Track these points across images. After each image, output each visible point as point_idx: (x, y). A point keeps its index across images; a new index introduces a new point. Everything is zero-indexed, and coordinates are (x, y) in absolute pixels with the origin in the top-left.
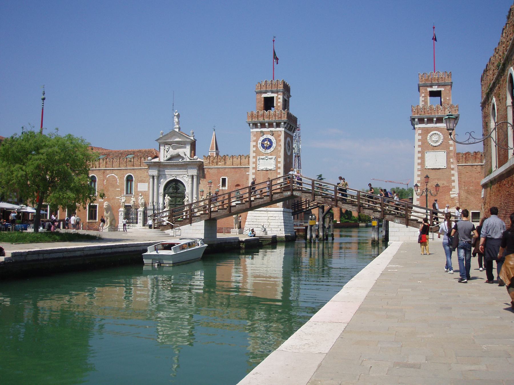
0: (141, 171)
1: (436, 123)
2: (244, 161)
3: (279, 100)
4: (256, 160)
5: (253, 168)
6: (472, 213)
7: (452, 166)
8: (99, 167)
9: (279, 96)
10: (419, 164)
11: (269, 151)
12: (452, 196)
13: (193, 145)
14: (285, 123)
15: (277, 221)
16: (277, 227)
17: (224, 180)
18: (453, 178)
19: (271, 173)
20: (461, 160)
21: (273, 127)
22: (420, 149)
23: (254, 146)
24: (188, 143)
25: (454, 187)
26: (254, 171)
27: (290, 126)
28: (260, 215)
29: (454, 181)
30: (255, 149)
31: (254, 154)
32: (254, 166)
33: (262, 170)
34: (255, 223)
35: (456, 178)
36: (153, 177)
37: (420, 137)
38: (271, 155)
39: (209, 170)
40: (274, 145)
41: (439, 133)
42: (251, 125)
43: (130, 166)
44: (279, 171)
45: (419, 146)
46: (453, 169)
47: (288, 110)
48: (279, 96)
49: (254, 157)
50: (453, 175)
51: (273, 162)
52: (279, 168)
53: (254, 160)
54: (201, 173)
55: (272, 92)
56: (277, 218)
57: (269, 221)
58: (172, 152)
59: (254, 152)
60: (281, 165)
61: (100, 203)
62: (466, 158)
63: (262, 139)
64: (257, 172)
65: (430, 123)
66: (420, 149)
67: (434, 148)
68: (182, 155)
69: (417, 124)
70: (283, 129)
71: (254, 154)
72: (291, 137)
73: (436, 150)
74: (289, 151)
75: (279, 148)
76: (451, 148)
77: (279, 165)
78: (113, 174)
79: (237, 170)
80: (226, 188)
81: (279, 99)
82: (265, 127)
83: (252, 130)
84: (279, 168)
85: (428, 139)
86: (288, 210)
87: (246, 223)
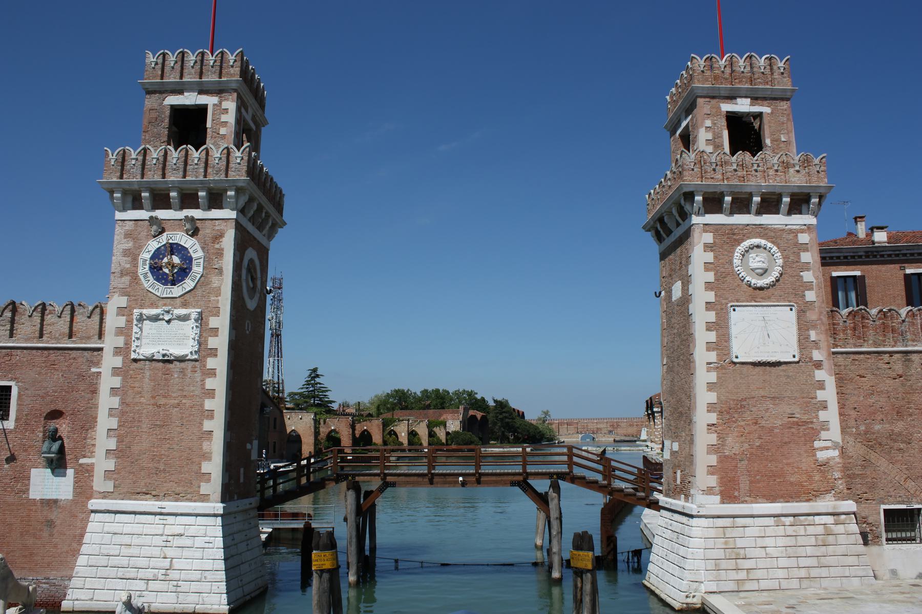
1: (759, 213)
3: (224, 118)
4: (129, 322)
5: (117, 351)
6: (885, 510)
7: (817, 355)
9: (225, 105)
10: (710, 347)
11: (177, 291)
12: (822, 456)
14: (239, 191)
15: (198, 554)
16: (196, 575)
18: (821, 395)
19: (183, 372)
20: (842, 336)
21: (197, 207)
22: (711, 296)
25: (825, 426)
26: (118, 362)
27: (260, 208)
28: (137, 529)
29: (824, 406)
31: (123, 301)
32: (120, 342)
33: (151, 360)
34: (114, 561)
35: (829, 395)
37: (710, 257)
38: (185, 305)
40: (197, 269)
41: (769, 245)
42: (117, 195)
44: (211, 363)
45: (709, 286)
46: (818, 365)
47: (255, 147)
48: (225, 105)
49: (121, 311)
50: (821, 385)
51: (190, 329)
52: (213, 353)
53: (122, 321)
55: (203, 90)
56: (199, 542)
57: (170, 552)
60: (221, 342)
62: (854, 329)
63: (153, 245)
65: (740, 212)
66: (711, 296)
67: (758, 295)
69: (698, 214)
70: (233, 214)
71: (123, 301)
72: (263, 253)
73: (764, 299)
74: (251, 298)
75: (215, 281)
76: (810, 296)
77: (212, 342)
79: (53, 356)
81: (223, 114)
82: (167, 205)
83: (119, 215)
84: (213, 353)
85: (736, 261)
86: (245, 503)
87: (82, 560)
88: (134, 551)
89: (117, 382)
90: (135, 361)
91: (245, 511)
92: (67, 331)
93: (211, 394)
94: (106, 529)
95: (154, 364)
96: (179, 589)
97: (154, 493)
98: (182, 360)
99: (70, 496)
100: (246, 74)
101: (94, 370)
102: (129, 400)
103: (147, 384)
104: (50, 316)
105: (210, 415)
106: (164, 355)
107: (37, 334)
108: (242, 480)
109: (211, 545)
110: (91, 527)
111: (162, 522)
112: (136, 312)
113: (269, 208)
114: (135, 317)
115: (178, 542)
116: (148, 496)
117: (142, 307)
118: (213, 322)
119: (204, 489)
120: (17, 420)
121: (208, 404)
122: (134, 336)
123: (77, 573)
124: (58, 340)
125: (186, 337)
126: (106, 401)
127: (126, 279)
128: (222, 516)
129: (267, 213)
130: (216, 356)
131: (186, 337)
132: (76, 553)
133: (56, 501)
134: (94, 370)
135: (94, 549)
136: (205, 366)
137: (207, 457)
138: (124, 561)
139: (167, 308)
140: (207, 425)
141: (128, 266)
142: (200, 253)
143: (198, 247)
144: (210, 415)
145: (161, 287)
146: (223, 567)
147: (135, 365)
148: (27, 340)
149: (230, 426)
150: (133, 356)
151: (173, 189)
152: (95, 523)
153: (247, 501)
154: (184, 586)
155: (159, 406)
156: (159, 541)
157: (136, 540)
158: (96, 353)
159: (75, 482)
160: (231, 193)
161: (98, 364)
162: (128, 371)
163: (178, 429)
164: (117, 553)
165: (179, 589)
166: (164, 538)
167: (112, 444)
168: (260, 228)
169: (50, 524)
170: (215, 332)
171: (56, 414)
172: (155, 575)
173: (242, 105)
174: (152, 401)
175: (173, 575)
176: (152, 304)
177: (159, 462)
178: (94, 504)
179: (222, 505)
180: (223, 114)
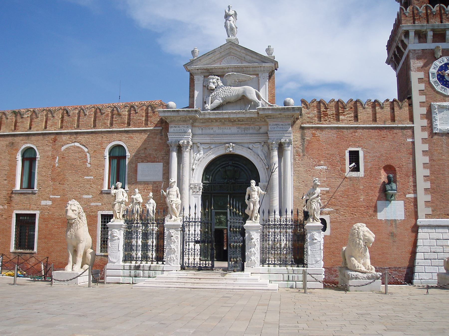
17: (354, 156)
23: (420, 80)
30: (422, 86)
31: (423, 98)
39: (318, 133)
58: (225, 91)
59: (421, 92)
61: (42, 209)
78: (77, 144)
79: (384, 132)
80: (361, 173)
89: (426, 147)
90: (436, 133)
92: (389, 116)
94: (431, 237)
102: (434, 158)
120: (365, 171)
123: (418, 263)
124: (385, 122)
126: (421, 159)
135: (428, 249)
147: (436, 137)
159: (406, 209)
167: (428, 185)
169: (392, 235)
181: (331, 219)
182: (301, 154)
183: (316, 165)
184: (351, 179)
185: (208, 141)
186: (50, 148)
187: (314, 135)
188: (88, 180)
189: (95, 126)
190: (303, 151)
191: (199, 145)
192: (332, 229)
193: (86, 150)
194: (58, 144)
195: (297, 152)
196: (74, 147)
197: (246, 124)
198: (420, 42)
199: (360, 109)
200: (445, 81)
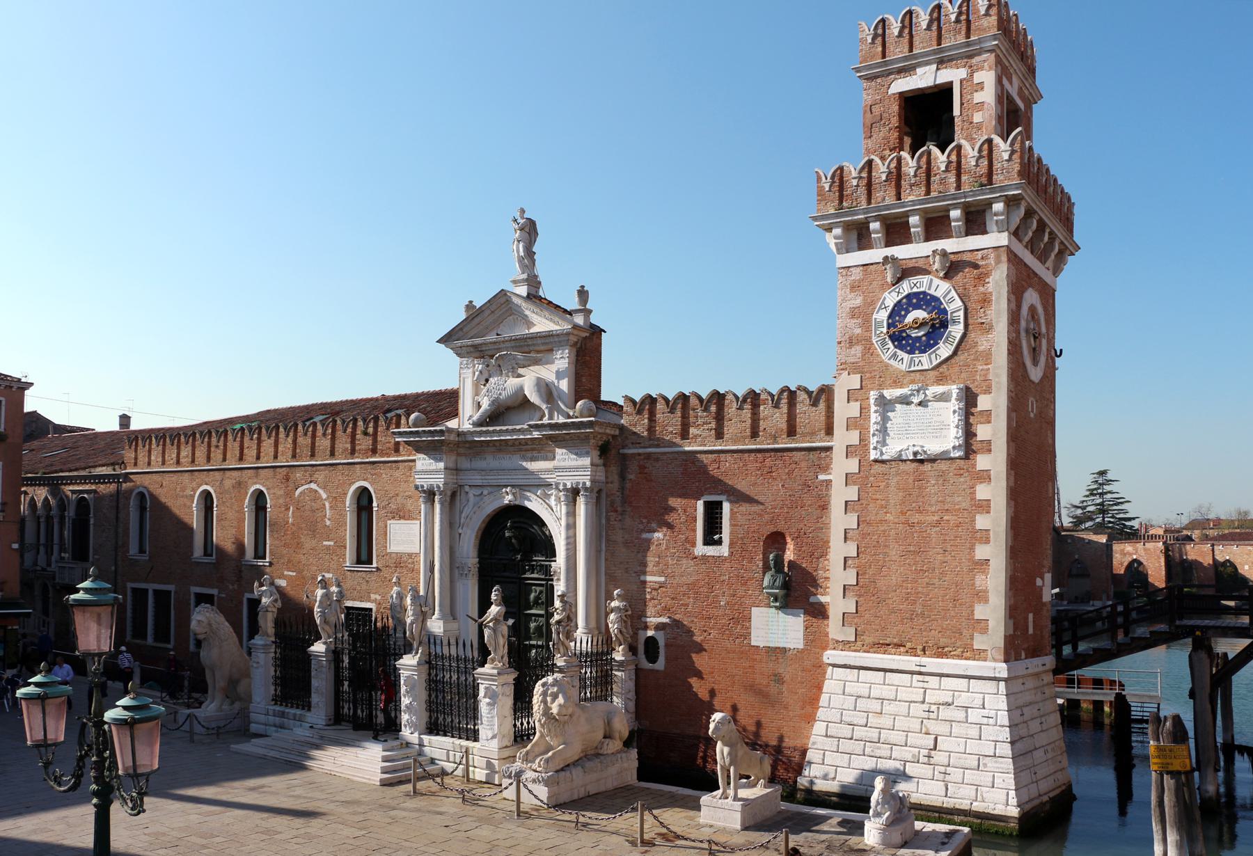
0: (397, 474)
2: (808, 415)
5: (850, 451)
8: (276, 457)
11: (925, 361)
13: (587, 349)
24: (560, 345)
28: (887, 692)
31: (855, 381)
32: (854, 438)
33: (899, 459)
34: (860, 732)
36: (430, 494)
38: (941, 380)
43: (365, 454)
52: (987, 447)
53: (854, 409)
54: (616, 478)
57: (934, 727)
58: (506, 385)
60: (994, 431)
63: (891, 299)
64: (872, 472)
68: (534, 398)
71: (855, 381)
74: (1035, 362)
78: (313, 486)
80: (724, 550)
84: (987, 447)
86: (1035, 664)
87: (819, 728)
88: (886, 721)
90: (876, 461)
91: (1037, 675)
92: (784, 426)
93: (984, 506)
95: (902, 466)
96: (948, 778)
97: (909, 645)
98: (943, 457)
99: (801, 646)
100: (1006, 26)
101: (822, 477)
103: (895, 497)
104: (762, 408)
105: (984, 537)
106: (915, 454)
107: (748, 432)
108: (1031, 631)
109: (991, 721)
110: (828, 686)
111: (921, 684)
112: (873, 395)
113: (1053, 225)
114: (872, 401)
115: (945, 713)
116: (902, 649)
117: (881, 386)
118: (983, 402)
119: (979, 642)
120: (731, 545)
121: (982, 522)
122: (873, 428)
124: (775, 438)
125: (944, 426)
126: (839, 521)
127: (857, 350)
128: (1005, 680)
129: (1051, 233)
130: (990, 451)
131: (944, 426)
132: (811, 719)
133: (784, 650)
134: (822, 477)
136: (974, 466)
137: (982, 596)
138: (873, 734)
139: (915, 387)
140: (981, 552)
141: (858, 331)
142: (958, 303)
143: (953, 293)
144: (984, 537)
145: (906, 356)
146: (1009, 753)
147: (877, 466)
148: (735, 442)
149: (1014, 552)
150: (873, 455)
151: (914, 212)
152: (833, 682)
153: (1037, 661)
154: (956, 774)
155: (912, 525)
156: (917, 710)
157: (888, 708)
158: (823, 455)
160: (998, 207)
161: (826, 469)
162: (867, 477)
163: (939, 557)
164: (863, 722)
165: (948, 778)
166: (926, 707)
168: (1042, 258)
169: (779, 679)
170: (987, 416)
171: (776, 540)
172: (914, 756)
173: (1003, 74)
174: (902, 519)
175: (939, 757)
176: (895, 382)
177: (914, 602)
178: (830, 656)
179: (1004, 665)
180: (978, 91)
181: (667, 639)
182: (619, 509)
183: (643, 531)
184: (704, 557)
185: (479, 482)
186: (282, 492)
187: (642, 467)
188: (328, 547)
189: (332, 454)
190: (624, 501)
191: (467, 488)
192: (667, 658)
193: (324, 496)
194: (291, 485)
195: (612, 503)
196: (311, 490)
197: (533, 450)
198: (860, 249)
199: (731, 409)
200: (904, 338)
